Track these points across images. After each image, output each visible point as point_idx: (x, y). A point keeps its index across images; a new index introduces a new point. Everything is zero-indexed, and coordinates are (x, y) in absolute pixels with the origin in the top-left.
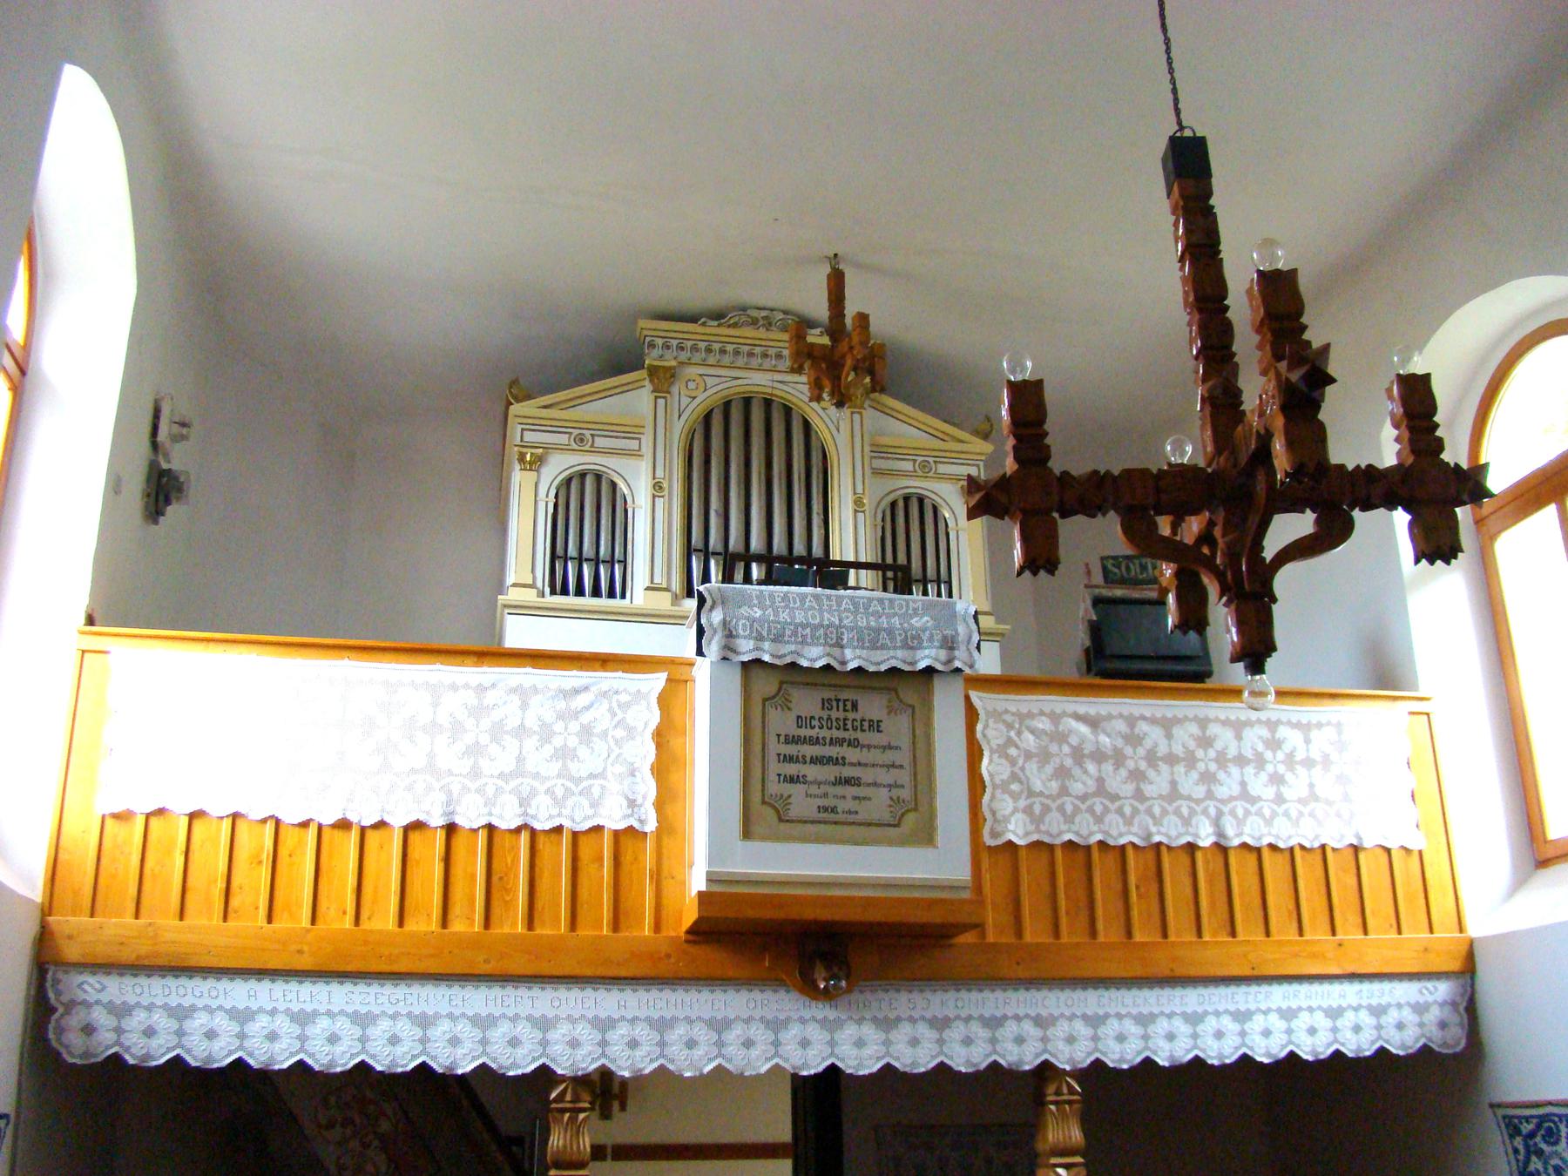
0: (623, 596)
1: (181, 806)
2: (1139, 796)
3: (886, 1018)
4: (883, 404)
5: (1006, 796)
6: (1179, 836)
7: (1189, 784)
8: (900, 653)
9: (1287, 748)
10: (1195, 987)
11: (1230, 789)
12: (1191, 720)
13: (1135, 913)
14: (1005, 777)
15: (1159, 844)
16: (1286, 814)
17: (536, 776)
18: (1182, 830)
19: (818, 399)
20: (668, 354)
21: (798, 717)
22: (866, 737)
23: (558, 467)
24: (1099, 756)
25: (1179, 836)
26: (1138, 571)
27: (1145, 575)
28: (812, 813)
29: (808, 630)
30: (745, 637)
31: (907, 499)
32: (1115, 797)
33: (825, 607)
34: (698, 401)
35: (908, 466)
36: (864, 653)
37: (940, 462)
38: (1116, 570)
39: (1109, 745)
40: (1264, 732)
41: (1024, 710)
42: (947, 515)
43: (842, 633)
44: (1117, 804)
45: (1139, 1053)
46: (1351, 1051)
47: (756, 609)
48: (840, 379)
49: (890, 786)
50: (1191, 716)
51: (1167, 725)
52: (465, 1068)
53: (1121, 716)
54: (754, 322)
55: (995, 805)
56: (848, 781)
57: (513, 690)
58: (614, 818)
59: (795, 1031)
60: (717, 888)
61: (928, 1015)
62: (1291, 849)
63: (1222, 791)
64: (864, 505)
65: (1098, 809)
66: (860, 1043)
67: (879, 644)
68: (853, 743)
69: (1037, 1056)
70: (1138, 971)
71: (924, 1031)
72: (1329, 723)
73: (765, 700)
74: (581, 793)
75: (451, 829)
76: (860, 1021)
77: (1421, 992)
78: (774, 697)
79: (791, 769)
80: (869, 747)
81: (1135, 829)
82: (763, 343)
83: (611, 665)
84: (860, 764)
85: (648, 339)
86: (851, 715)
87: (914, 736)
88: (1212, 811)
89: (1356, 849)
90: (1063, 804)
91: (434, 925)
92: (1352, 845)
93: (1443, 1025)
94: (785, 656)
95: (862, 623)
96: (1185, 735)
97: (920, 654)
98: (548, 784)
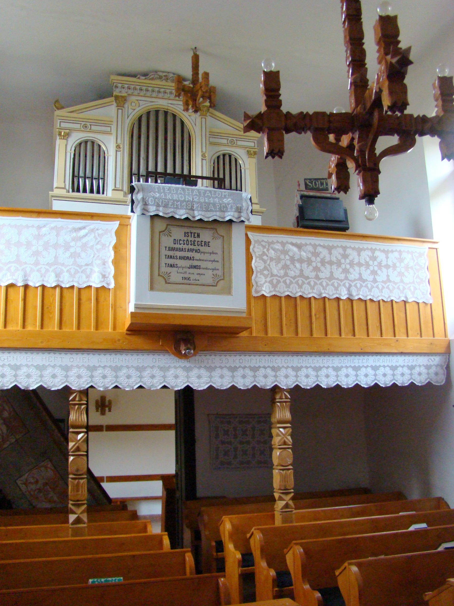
0: (103, 193)
2: (317, 277)
3: (210, 366)
4: (215, 115)
5: (262, 276)
6: (333, 294)
7: (338, 273)
8: (218, 214)
9: (379, 260)
10: (338, 356)
11: (355, 276)
12: (339, 247)
13: (314, 326)
14: (261, 268)
15: (325, 298)
16: (377, 287)
17: (63, 265)
18: (335, 292)
19: (187, 110)
20: (123, 90)
21: (174, 240)
22: (202, 249)
24: (301, 261)
25: (333, 294)
26: (320, 185)
27: (322, 187)
28: (180, 280)
29: (179, 203)
30: (152, 205)
31: (224, 155)
32: (307, 278)
33: (187, 193)
34: (136, 111)
35: (225, 141)
36: (203, 213)
37: (238, 140)
38: (311, 185)
39: (305, 256)
40: (370, 253)
41: (270, 241)
42: (241, 163)
43: (194, 204)
44: (308, 281)
45: (314, 382)
46: (400, 384)
47: (157, 193)
48: (196, 100)
49: (213, 269)
50: (339, 245)
51: (330, 249)
52: (33, 387)
53: (310, 244)
54: (160, 78)
55: (257, 279)
56: (195, 267)
57: (52, 228)
58: (96, 282)
59: (172, 372)
60: (138, 311)
61: (228, 366)
62: (379, 301)
63: (351, 277)
64: (205, 157)
65: (300, 282)
66: (199, 377)
67: (209, 209)
68: (197, 251)
69: (273, 383)
70: (315, 349)
71: (226, 372)
72: (396, 251)
73: (160, 232)
74: (82, 272)
75: (26, 287)
76: (200, 368)
77: (428, 361)
78: (164, 231)
79: (171, 261)
80: (204, 253)
81: (315, 291)
82: (165, 87)
83: (95, 218)
84: (200, 260)
85: (115, 84)
86: (197, 239)
87: (223, 248)
88: (347, 285)
89: (405, 302)
90: (286, 280)
91: (19, 328)
92: (403, 300)
93: (436, 374)
94: (169, 213)
95: (202, 201)
96: (337, 253)
97: (227, 214)
98: (68, 268)
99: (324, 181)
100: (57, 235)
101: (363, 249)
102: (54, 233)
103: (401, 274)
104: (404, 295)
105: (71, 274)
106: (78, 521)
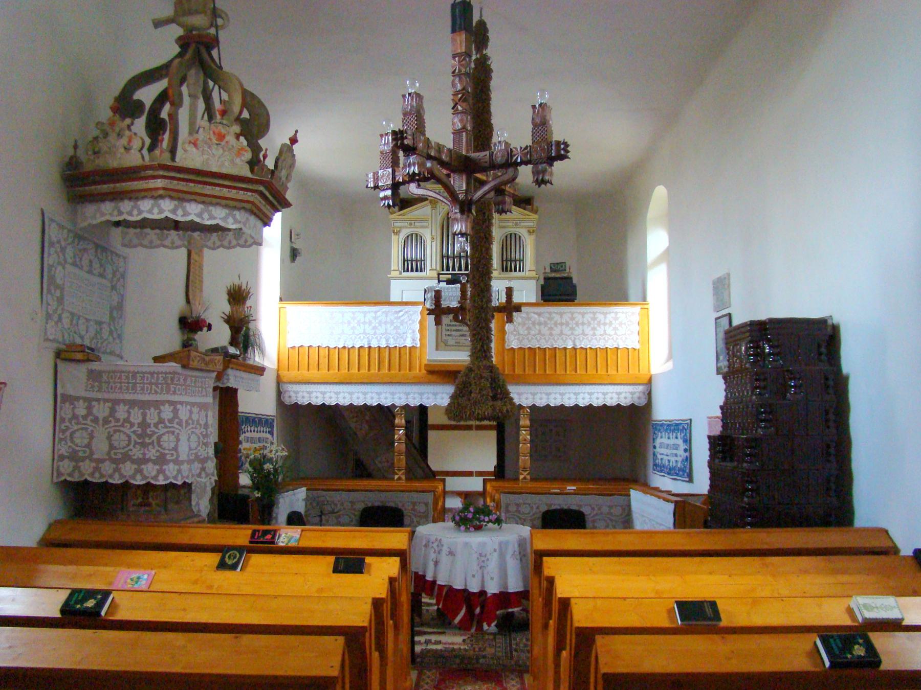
1: (306, 345)
2: (551, 334)
7: (566, 330)
9: (598, 320)
16: (596, 339)
17: (390, 334)
23: (405, 233)
24: (540, 324)
31: (511, 234)
35: (511, 224)
40: (592, 315)
51: (561, 314)
52: (375, 404)
57: (383, 312)
58: (409, 344)
63: (576, 333)
65: (539, 338)
72: (613, 312)
75: (370, 347)
79: (449, 333)
88: (573, 339)
89: (617, 348)
91: (367, 371)
93: (639, 398)
96: (566, 317)
99: (564, 264)
100: (386, 316)
101: (587, 313)
102: (384, 315)
103: (615, 329)
104: (616, 344)
105: (394, 339)
106: (399, 479)
